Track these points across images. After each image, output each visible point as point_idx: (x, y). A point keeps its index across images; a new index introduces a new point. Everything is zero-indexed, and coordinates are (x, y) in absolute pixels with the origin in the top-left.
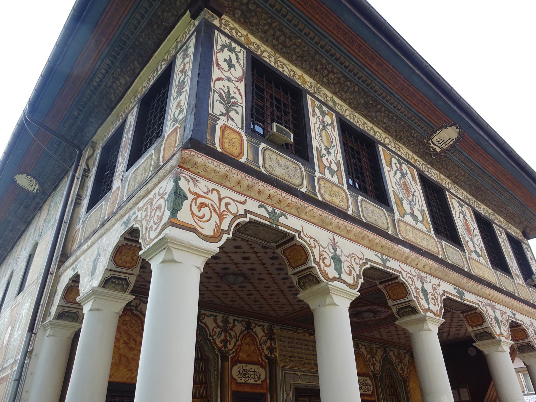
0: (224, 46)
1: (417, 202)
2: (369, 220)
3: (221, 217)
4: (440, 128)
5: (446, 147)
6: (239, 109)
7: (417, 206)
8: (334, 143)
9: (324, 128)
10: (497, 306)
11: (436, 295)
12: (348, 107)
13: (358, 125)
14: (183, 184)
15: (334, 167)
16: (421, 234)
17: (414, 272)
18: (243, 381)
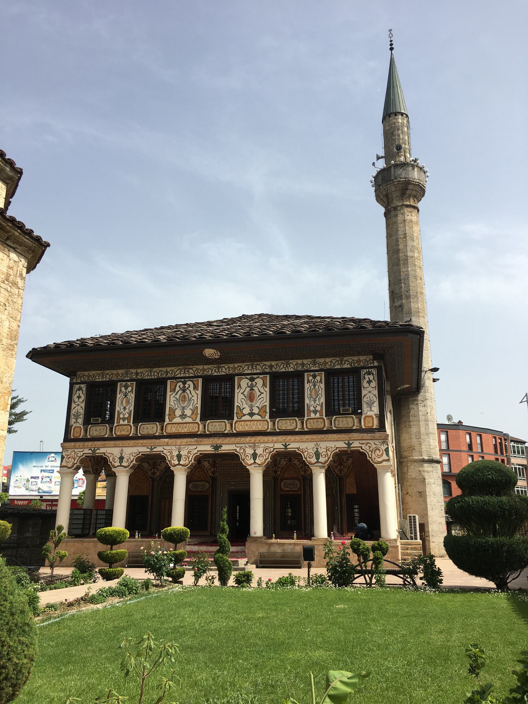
0: (77, 390)
1: (192, 403)
2: (144, 433)
3: (75, 459)
4: (202, 352)
5: (219, 354)
6: (81, 416)
7: (191, 407)
8: (130, 401)
9: (126, 396)
10: (262, 445)
11: (189, 455)
12: (147, 369)
13: (153, 377)
14: (64, 454)
15: (127, 416)
16: (185, 425)
17: (173, 448)
18: (195, 490)
